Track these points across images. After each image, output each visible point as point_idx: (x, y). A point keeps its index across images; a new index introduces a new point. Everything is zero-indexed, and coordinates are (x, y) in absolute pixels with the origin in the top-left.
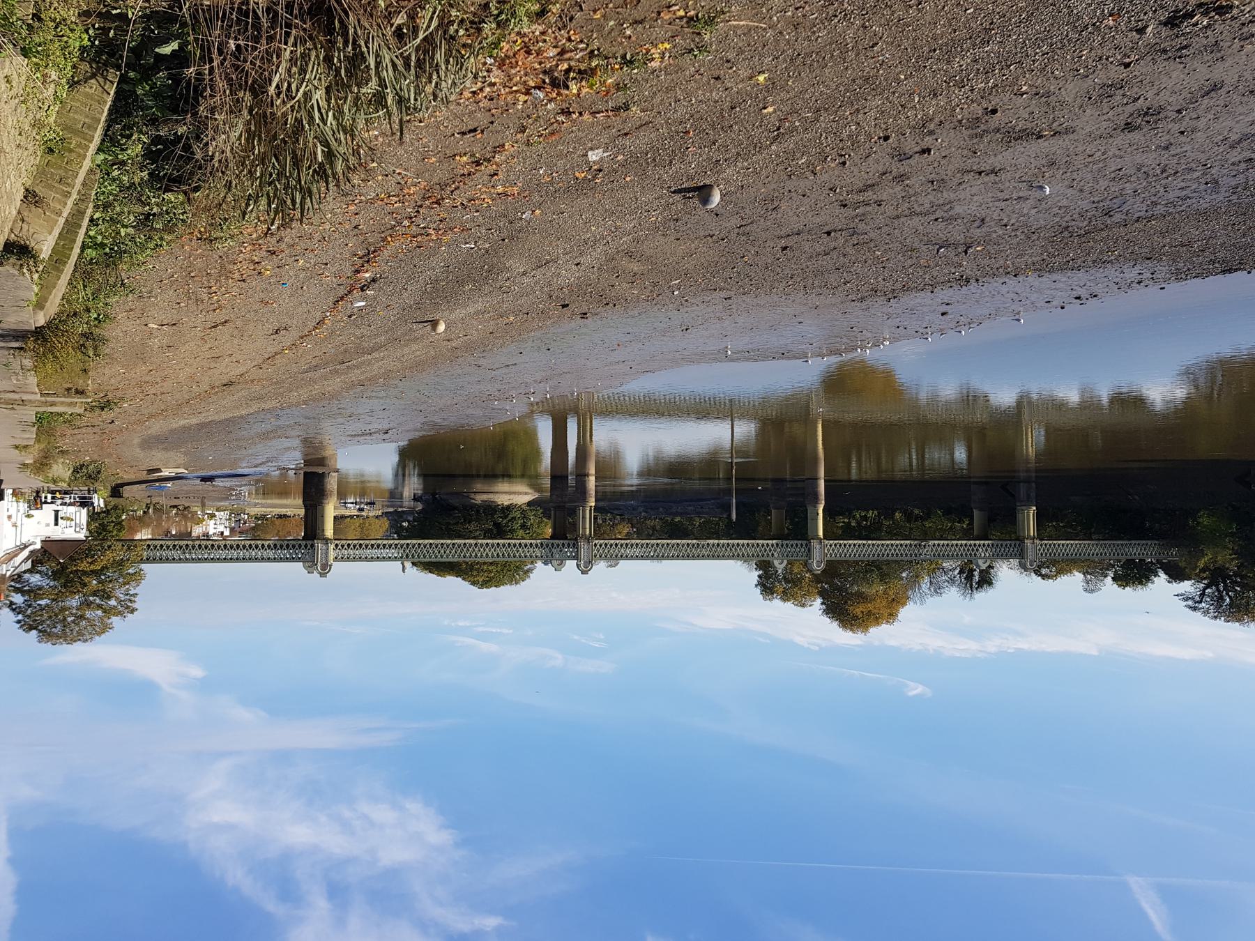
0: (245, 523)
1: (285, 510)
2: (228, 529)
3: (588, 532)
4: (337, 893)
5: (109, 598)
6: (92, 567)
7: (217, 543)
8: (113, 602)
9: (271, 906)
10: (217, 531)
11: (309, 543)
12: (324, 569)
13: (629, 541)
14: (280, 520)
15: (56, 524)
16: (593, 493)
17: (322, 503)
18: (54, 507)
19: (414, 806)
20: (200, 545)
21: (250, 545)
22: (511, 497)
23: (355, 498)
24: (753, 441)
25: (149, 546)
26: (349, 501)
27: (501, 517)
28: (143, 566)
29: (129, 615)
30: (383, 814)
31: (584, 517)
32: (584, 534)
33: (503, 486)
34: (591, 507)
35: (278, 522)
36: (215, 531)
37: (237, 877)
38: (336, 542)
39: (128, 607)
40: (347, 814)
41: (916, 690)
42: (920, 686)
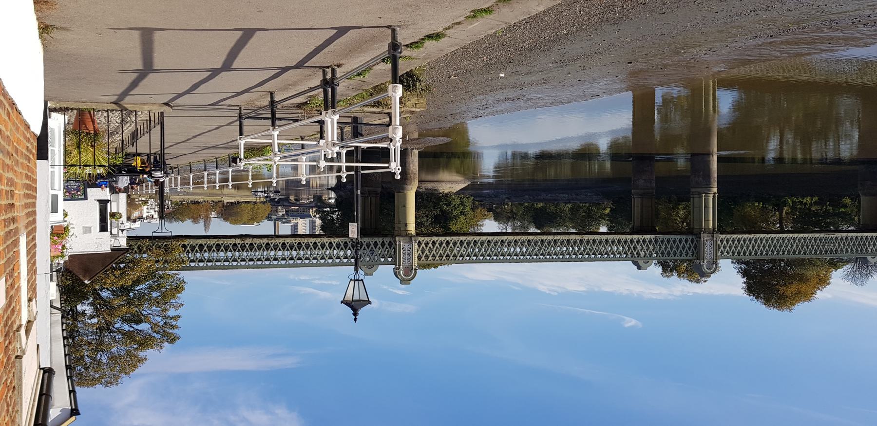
1: (198, 197)
2: (157, 213)
3: (711, 226)
5: (139, 322)
6: (120, 284)
7: (273, 241)
8: (144, 327)
10: (149, 215)
11: (387, 240)
12: (407, 274)
13: (752, 236)
14: (194, 206)
15: (103, 228)
17: (403, 189)
18: (104, 193)
20: (251, 244)
21: (315, 243)
22: (453, 185)
23: (264, 187)
24: (630, 134)
25: (184, 246)
26: (259, 190)
27: (445, 204)
28: (184, 275)
29: (166, 344)
31: (706, 207)
32: (707, 231)
33: (444, 175)
34: (715, 193)
35: (193, 207)
36: (147, 214)
38: (421, 239)
39: (165, 334)
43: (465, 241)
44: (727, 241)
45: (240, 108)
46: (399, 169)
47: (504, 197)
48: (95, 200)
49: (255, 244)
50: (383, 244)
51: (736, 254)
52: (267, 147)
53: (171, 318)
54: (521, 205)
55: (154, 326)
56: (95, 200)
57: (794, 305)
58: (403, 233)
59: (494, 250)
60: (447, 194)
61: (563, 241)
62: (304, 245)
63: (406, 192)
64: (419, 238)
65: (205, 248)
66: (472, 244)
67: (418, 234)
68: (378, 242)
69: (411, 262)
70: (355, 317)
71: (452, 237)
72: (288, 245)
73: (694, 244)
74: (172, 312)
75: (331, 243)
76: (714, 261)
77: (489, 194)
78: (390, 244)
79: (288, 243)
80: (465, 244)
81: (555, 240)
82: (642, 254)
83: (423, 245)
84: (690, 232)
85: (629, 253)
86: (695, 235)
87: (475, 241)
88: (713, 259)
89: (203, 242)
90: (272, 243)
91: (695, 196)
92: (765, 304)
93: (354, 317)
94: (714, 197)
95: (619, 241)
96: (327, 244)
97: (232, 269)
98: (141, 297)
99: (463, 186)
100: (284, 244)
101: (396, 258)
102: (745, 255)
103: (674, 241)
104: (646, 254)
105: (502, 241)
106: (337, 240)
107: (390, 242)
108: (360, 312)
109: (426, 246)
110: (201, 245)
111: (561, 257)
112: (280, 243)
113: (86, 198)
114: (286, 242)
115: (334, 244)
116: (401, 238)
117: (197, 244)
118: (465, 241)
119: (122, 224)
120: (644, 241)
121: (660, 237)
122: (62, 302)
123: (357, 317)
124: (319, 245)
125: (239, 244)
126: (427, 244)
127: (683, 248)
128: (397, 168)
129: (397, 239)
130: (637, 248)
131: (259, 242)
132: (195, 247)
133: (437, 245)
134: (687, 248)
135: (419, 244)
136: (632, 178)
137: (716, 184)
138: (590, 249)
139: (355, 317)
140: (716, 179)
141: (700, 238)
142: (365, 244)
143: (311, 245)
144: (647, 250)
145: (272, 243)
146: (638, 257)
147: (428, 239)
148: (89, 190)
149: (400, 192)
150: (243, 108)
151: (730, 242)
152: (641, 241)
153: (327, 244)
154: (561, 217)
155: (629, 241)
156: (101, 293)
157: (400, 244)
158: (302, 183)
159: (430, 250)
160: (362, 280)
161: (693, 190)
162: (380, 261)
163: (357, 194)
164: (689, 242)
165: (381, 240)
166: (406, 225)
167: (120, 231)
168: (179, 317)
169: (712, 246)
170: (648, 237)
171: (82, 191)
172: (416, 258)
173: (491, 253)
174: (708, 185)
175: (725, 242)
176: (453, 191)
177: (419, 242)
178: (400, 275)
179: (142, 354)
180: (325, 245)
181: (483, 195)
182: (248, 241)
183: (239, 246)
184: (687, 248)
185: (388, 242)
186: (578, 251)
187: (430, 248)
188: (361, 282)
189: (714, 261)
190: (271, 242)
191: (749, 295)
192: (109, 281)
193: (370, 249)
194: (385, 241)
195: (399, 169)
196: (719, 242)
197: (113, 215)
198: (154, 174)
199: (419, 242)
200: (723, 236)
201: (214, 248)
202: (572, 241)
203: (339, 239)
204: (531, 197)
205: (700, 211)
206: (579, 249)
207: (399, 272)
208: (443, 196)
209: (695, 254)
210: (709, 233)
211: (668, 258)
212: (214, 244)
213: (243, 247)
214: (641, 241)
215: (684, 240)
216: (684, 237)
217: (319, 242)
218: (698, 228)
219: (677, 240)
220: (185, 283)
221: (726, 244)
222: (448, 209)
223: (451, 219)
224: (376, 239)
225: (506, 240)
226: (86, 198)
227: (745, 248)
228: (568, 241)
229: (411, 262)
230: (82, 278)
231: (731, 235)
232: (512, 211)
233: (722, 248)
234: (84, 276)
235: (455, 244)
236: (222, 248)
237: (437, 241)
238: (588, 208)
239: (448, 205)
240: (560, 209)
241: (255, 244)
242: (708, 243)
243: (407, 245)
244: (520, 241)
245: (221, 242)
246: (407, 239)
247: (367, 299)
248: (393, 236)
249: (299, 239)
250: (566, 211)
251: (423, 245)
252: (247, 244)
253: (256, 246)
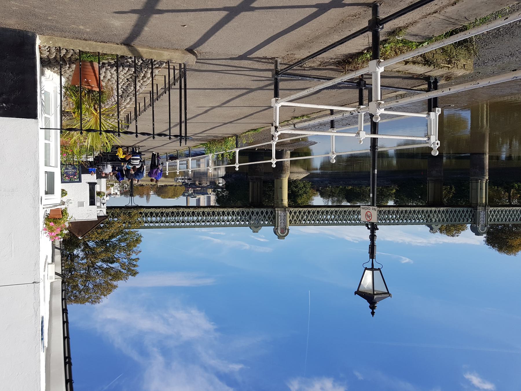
0: (126, 188)
2: (119, 191)
3: (484, 201)
4: (165, 352)
6: (101, 238)
7: (197, 210)
9: (135, 356)
11: (269, 210)
12: (282, 232)
13: (511, 208)
15: (92, 203)
16: (488, 168)
17: (281, 177)
19: (194, 312)
20: (183, 212)
21: (223, 212)
22: (299, 175)
23: (182, 177)
25: (141, 213)
26: (179, 178)
27: (295, 187)
28: (141, 231)
30: (181, 315)
31: (481, 189)
32: (481, 205)
35: (140, 188)
36: (114, 192)
37: (118, 342)
38: (292, 209)
39: (129, 270)
40: (165, 315)
41: (406, 260)
42: (407, 259)
43: (320, 211)
44: (494, 212)
45: (276, 61)
46: (437, 144)
47: (327, 182)
48: (86, 182)
49: (186, 212)
51: (496, 220)
52: (229, 137)
53: (134, 260)
54: (338, 187)
55: (123, 265)
56: (86, 182)
57: (518, 251)
58: (280, 206)
59: (349, 217)
60: (295, 180)
61: (385, 212)
62: (216, 213)
63: (282, 179)
64: (291, 209)
65: (154, 214)
66: (325, 213)
67: (290, 206)
68: (264, 211)
69: (285, 224)
70: (373, 311)
71: (312, 209)
72: (206, 213)
73: (472, 213)
74: (133, 256)
75: (233, 212)
76: (486, 225)
77: (317, 181)
78: (272, 213)
79: (206, 211)
80: (320, 213)
81: (380, 211)
82: (434, 220)
83: (293, 213)
84: (470, 206)
85: (425, 220)
86: (473, 207)
87: (327, 211)
88: (485, 224)
90: (196, 212)
91: (473, 182)
92: (499, 251)
93: (371, 310)
94: (486, 182)
95: (423, 211)
96: (231, 213)
97: (171, 228)
98: (114, 246)
99: (305, 175)
100: (203, 212)
101: (275, 222)
102: (506, 221)
103: (459, 212)
104: (436, 220)
105: (345, 211)
106: (237, 210)
107: (271, 211)
108: (379, 305)
109: (295, 214)
110: (151, 213)
111: (384, 221)
112: (201, 212)
113: (80, 181)
114: (205, 211)
115: (236, 213)
116: (279, 209)
117: (149, 212)
118: (320, 211)
119: (103, 199)
120: (439, 211)
122: (63, 261)
123: (374, 311)
124: (226, 213)
125: (175, 212)
126: (295, 213)
127: (465, 216)
128: (436, 142)
129: (276, 209)
130: (430, 216)
131: (188, 211)
132: (147, 214)
133: (302, 213)
134: (463, 216)
135: (291, 213)
136: (428, 170)
137: (488, 173)
138: (407, 216)
139: (373, 311)
140: (488, 170)
141: (477, 210)
142: (255, 213)
143: (221, 213)
144: (437, 218)
145: (196, 212)
146: (431, 222)
147: (296, 209)
148: (82, 175)
149: (278, 179)
150: (279, 61)
151: (496, 212)
152: (437, 211)
153: (231, 213)
154: (363, 195)
155: (429, 211)
156: (88, 243)
157: (278, 213)
158: (236, 169)
159: (298, 217)
160: (379, 269)
161: (472, 178)
162: (265, 223)
163: (374, 174)
164: (469, 212)
165: (265, 210)
166: (282, 200)
167: (102, 204)
168: (138, 259)
169: (485, 215)
170: (442, 209)
171: (78, 176)
172: (288, 222)
173: (346, 219)
174: (483, 175)
175: (493, 212)
176: (299, 178)
177: (291, 211)
178: (278, 233)
179: (115, 283)
180: (230, 213)
181: (314, 181)
182: (181, 210)
183: (175, 213)
184: (463, 216)
185: (270, 211)
186: (395, 218)
187: (297, 215)
188: (379, 271)
189: (486, 225)
190: (196, 211)
191: (488, 245)
192: (94, 236)
193: (258, 216)
194: (268, 211)
195: (437, 144)
196: (489, 213)
197: (99, 194)
198: (133, 162)
199: (291, 211)
200: (492, 208)
201: (159, 214)
202: (391, 212)
203: (238, 209)
204: (344, 183)
205: (477, 192)
206: (400, 216)
207: (278, 231)
208: (293, 181)
209: (473, 220)
210: (483, 206)
211: (455, 223)
212: (159, 212)
213: (178, 214)
214: (437, 211)
215: (465, 211)
216: (465, 209)
217: (226, 211)
218: (476, 203)
219: (461, 211)
220: (142, 237)
221: (493, 213)
222: (296, 190)
223: (298, 196)
225: (347, 211)
226: (80, 181)
227: (506, 216)
228: (389, 211)
229: (285, 224)
230: (77, 235)
231: (497, 208)
232: (331, 191)
233: (491, 216)
234: (78, 234)
235: (314, 213)
236: (165, 214)
237: (302, 211)
238: (381, 190)
239: (296, 187)
240: (363, 190)
241: (186, 212)
242: (482, 213)
243: (282, 213)
244: (348, 211)
246: (283, 209)
247: (387, 291)
248: (273, 207)
249: (213, 209)
250: (366, 191)
251: (293, 213)
252: (180, 212)
253: (186, 213)
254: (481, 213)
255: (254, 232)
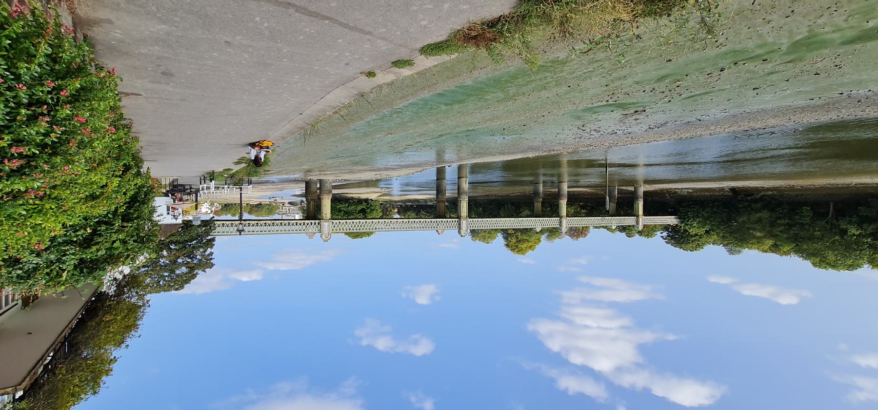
11: (317, 221)
50: (315, 224)
58: (325, 218)
78: (319, 223)
89: (224, 222)
116: (324, 221)
121: (449, 220)
126: (336, 224)
182: (248, 222)
224: (311, 221)
245: (233, 222)
251: (335, 224)
254: (464, 223)
255: (310, 238)
